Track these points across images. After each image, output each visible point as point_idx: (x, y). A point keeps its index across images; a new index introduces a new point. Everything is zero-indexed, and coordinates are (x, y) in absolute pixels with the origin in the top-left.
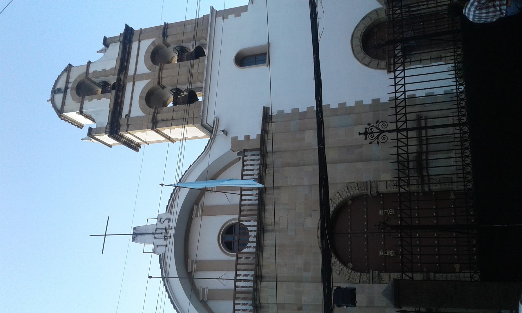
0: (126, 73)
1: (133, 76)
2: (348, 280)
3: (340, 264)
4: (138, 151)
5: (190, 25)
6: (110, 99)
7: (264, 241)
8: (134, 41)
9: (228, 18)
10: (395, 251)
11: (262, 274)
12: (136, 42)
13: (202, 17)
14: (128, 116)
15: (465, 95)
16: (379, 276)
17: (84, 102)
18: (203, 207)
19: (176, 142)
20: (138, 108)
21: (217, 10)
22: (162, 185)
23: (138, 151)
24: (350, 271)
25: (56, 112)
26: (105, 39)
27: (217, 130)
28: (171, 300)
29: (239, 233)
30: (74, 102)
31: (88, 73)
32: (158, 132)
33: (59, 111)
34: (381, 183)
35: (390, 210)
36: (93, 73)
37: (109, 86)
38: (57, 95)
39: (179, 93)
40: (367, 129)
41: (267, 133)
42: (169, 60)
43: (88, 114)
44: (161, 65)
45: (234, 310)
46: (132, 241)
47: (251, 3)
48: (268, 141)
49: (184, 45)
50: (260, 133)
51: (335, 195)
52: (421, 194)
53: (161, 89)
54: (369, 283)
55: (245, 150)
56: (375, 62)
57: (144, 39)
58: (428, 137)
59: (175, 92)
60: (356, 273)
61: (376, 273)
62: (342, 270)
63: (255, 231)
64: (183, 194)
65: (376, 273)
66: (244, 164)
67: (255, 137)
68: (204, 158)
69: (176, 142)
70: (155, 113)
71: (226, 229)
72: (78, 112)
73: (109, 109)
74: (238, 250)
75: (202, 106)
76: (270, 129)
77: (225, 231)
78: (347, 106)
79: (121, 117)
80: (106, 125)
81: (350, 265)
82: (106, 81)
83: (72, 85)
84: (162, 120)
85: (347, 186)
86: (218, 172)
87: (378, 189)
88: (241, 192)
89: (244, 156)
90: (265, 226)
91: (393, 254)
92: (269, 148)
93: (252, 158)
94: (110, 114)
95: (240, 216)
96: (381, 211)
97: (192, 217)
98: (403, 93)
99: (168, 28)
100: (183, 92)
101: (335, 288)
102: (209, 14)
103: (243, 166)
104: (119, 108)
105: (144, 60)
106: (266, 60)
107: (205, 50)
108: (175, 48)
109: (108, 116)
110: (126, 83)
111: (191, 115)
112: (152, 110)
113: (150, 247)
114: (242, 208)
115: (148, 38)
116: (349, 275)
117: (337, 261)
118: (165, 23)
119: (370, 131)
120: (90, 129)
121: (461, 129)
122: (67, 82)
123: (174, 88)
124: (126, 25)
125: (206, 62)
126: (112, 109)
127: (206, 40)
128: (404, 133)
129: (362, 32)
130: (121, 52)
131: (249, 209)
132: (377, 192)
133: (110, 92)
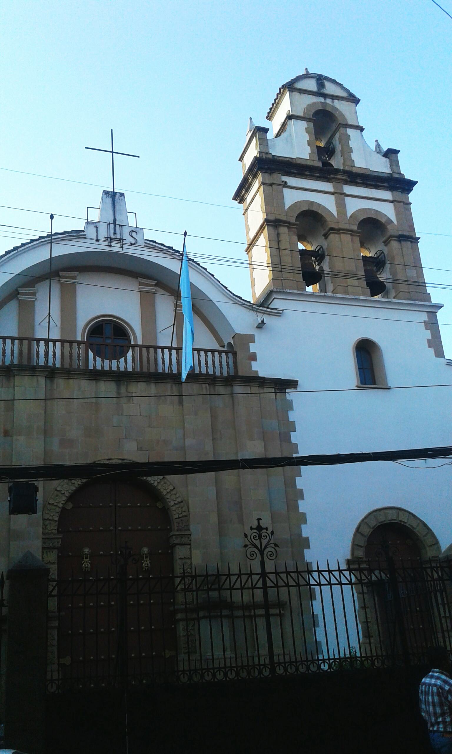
0: (347, 183)
1: (342, 192)
2: (47, 503)
3: (70, 491)
4: (234, 199)
5: (415, 275)
6: (309, 159)
7: (104, 381)
8: (393, 194)
9: (426, 329)
10: (89, 570)
11: (56, 379)
12: (392, 197)
13: (428, 292)
14: (285, 185)
15: (316, 672)
16: (54, 548)
17: (304, 121)
18: (153, 293)
19: (247, 254)
21: (437, 314)
22: (185, 234)
23: (234, 199)
24: (61, 505)
25: (290, 80)
26: (397, 152)
27: (264, 313)
28: (19, 247)
29: (115, 346)
31: (347, 128)
32: (262, 228)
33: (291, 85)
34: (188, 550)
35: (149, 564)
36: (347, 134)
37: (328, 157)
38: (315, 82)
39: (318, 258)
40: (265, 531)
41: (260, 385)
42: (365, 245)
43: (288, 127)
44: (359, 233)
45: (4, 339)
46: (104, 191)
47: (447, 362)
48: (249, 387)
49: (388, 266)
50: (259, 376)
51: (171, 484)
52: (172, 608)
53: (323, 232)
54: (43, 534)
55: (235, 354)
56: (362, 542)
57: (395, 208)
58: (254, 619)
59: (320, 252)
60: (57, 515)
61: (58, 542)
62: (62, 493)
63: (118, 368)
64: (173, 265)
65: (58, 542)
66: (216, 352)
67: (254, 369)
68: (225, 295)
69: (247, 254)
70: (288, 224)
71: (122, 327)
72: (291, 113)
73: (294, 158)
74: (91, 344)
75: (299, 292)
76: (266, 390)
77: (119, 325)
78: (299, 501)
79: (283, 175)
80: (271, 154)
81: (70, 506)
82: (336, 153)
83: (329, 104)
84: (278, 235)
85: (184, 501)
86: (203, 315)
87: (179, 546)
88: (174, 348)
89: (227, 353)
90: (126, 383)
91: (85, 567)
92: (238, 389)
93: (224, 364)
94: (288, 159)
95: (141, 347)
96: (148, 550)
97: (139, 278)
98: (318, 581)
99: (411, 242)
100: (318, 265)
101: (36, 483)
102: (431, 302)
103: (213, 352)
104: (296, 171)
105: (366, 209)
106: (365, 384)
107: (380, 295)
108: (383, 252)
109: (285, 156)
110: (332, 183)
111: (286, 275)
113: (95, 216)
114: (152, 350)
115: (398, 214)
116: (56, 504)
117: (76, 487)
118: (419, 238)
119: (263, 535)
120: (266, 130)
121: (265, 665)
122: (334, 97)
123: (326, 250)
124: (417, 182)
125: (362, 298)
126: (294, 162)
127: (394, 298)
128: (260, 584)
129: (405, 523)
130: (376, 174)
131: (150, 359)
132: (175, 545)
133: (320, 159)
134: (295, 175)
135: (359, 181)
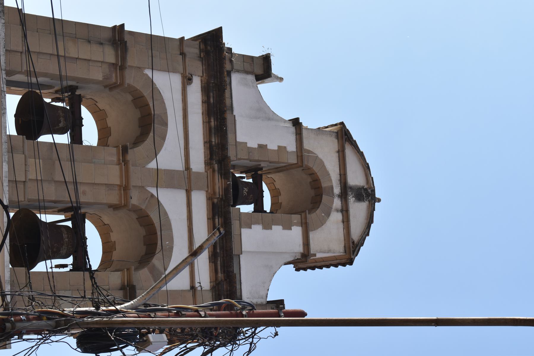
0: (209, 199)
6: (238, 140)
14: (187, 80)
20: (166, 95)
30: (320, 156)
79: (201, 82)
83: (333, 202)
84: (101, 44)
104: (212, 100)
110: (205, 172)
112: (131, 78)
122: (345, 211)
134: (206, 102)
135: (217, 220)
